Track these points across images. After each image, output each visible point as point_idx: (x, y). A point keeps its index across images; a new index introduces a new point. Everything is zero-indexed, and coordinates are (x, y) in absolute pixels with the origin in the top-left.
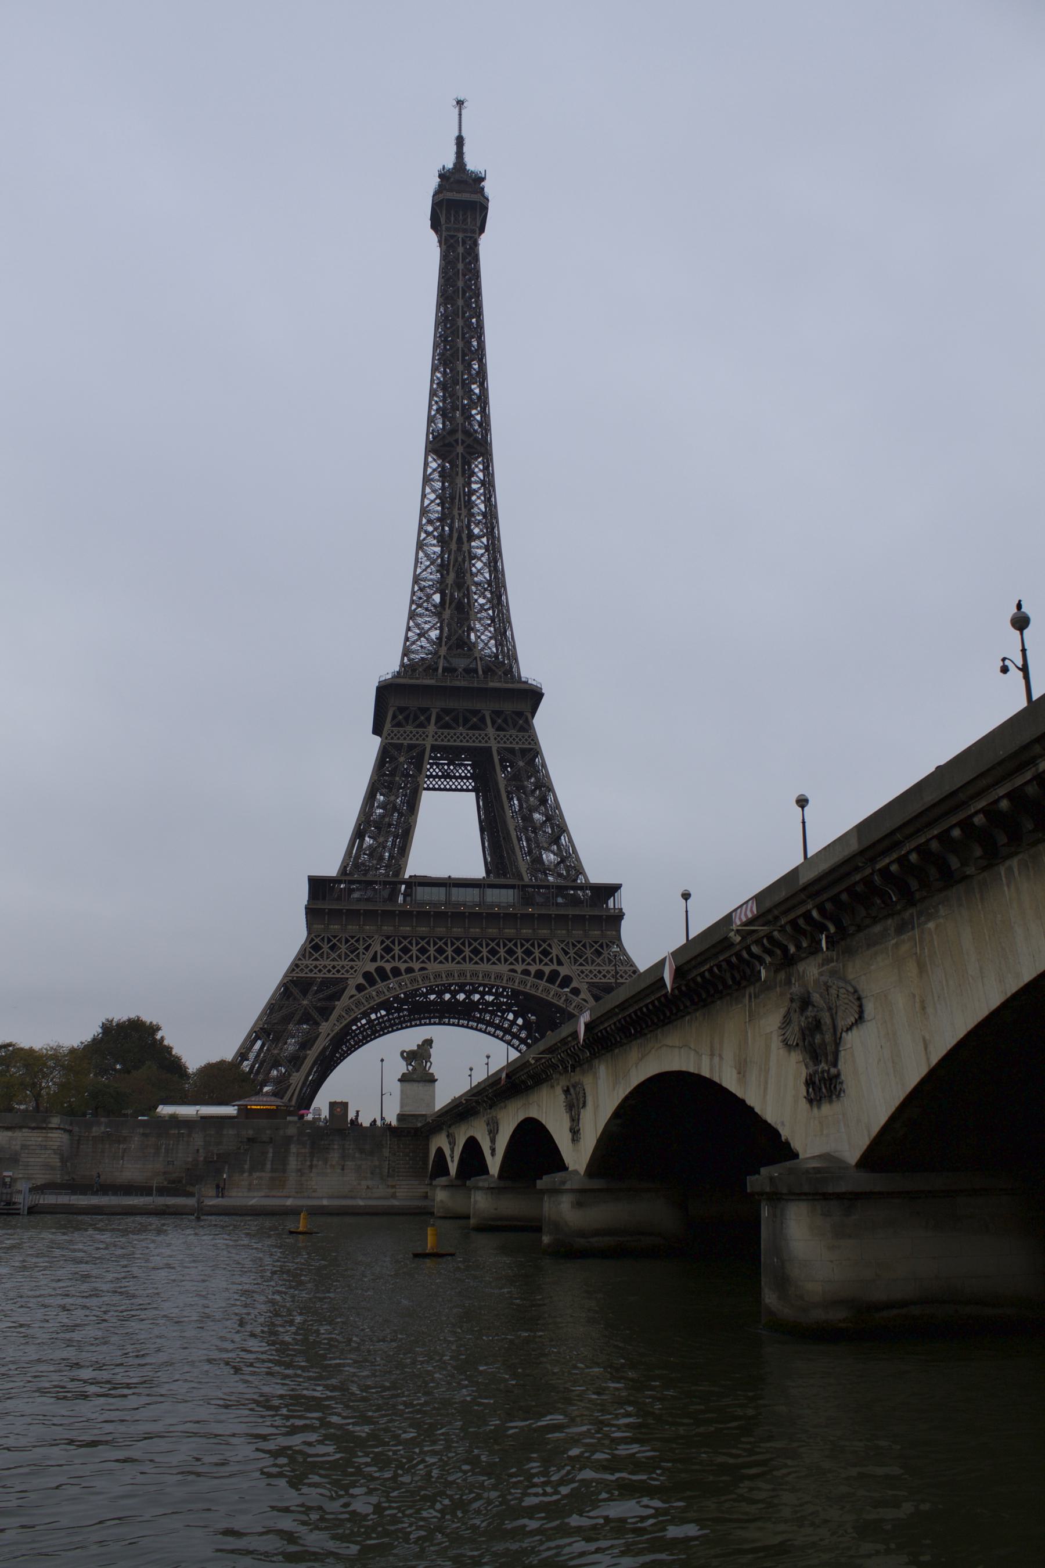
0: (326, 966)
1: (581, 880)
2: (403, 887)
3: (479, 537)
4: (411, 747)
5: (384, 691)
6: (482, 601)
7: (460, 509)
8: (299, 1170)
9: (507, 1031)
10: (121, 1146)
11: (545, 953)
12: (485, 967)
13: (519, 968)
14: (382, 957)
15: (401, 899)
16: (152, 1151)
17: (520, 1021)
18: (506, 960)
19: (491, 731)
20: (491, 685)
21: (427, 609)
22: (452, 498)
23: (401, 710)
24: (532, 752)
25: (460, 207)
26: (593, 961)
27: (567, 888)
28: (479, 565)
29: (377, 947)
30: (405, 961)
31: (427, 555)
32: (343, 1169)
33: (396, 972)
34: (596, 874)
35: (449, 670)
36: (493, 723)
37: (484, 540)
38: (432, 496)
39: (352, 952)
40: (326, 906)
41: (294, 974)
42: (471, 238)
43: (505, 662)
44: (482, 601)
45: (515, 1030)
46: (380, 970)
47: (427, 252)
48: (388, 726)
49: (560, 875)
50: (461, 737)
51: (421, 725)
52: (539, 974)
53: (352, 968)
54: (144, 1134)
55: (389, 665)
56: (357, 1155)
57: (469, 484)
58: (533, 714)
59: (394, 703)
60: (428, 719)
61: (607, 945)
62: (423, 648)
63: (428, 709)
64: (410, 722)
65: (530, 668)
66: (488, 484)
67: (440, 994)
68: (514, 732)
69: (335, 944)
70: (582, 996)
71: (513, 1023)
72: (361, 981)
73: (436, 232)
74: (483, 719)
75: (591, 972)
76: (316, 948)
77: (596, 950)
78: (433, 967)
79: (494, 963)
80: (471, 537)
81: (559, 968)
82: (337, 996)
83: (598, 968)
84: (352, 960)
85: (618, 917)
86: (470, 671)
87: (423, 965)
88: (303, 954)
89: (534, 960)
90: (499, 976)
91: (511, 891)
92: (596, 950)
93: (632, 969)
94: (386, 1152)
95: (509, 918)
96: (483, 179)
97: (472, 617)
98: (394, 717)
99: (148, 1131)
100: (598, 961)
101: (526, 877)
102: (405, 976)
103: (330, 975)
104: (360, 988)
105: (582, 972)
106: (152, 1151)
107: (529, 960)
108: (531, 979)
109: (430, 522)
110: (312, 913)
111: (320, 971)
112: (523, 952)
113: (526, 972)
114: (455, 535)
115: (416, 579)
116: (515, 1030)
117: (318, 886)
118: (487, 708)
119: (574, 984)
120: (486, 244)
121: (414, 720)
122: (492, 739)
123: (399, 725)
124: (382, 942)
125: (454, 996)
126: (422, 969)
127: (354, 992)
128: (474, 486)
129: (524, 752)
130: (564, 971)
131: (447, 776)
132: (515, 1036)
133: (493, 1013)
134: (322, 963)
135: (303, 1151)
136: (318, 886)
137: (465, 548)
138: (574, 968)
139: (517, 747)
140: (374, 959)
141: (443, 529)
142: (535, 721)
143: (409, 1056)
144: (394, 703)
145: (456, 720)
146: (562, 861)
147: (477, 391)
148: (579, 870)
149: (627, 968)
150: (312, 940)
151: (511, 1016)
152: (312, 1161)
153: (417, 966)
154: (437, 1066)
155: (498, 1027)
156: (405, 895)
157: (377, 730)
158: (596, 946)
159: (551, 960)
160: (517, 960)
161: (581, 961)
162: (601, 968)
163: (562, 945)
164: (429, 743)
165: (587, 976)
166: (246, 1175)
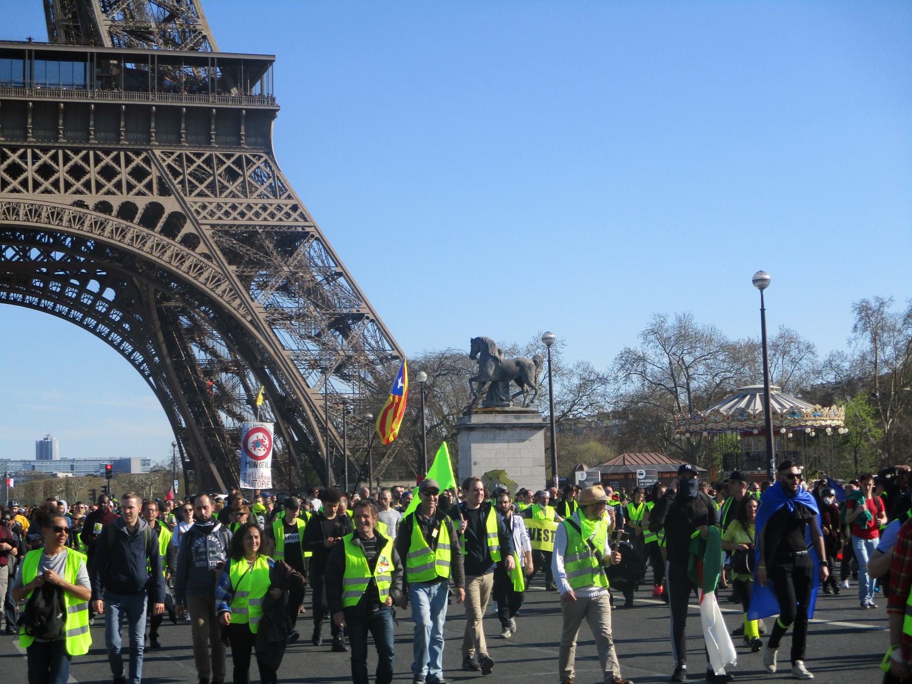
11: (140, 174)
12: (29, 197)
13: (91, 199)
18: (68, 186)
26: (223, 188)
27: (176, 61)
52: (127, 211)
61: (249, 161)
70: (202, 248)
75: (219, 206)
77: (229, 170)
79: (46, 191)
81: (162, 200)
83: (231, 201)
89: (118, 186)
90: (56, 214)
91: (79, 66)
92: (229, 170)
93: (291, 202)
100: (233, 187)
101: (107, 42)
107: (109, 186)
108: (113, 221)
112: (100, 173)
113: (104, 207)
130: (170, 205)
133: (46, 278)
149: (282, 201)
158: (229, 163)
159: (149, 186)
160: (87, 185)
161: (202, 187)
162: (235, 201)
163: (169, 161)
165: (212, 214)
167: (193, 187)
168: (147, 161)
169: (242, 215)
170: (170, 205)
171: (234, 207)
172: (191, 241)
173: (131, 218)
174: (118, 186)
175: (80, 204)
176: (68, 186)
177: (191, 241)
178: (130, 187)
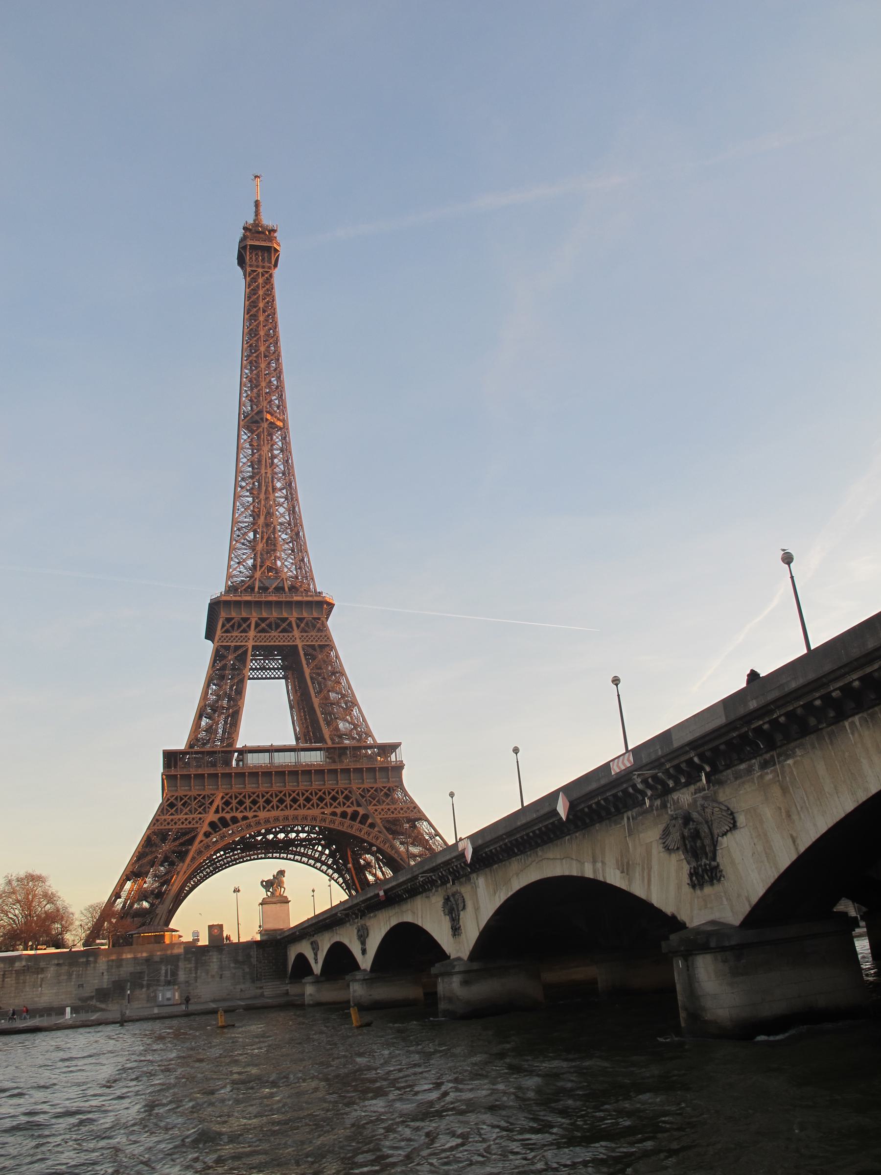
0: (181, 819)
1: (370, 741)
2: (236, 754)
3: (281, 490)
4: (237, 648)
5: (215, 607)
6: (284, 536)
7: (266, 468)
8: (187, 982)
9: (317, 860)
10: (40, 976)
11: (347, 798)
14: (223, 809)
15: (234, 763)
16: (66, 977)
17: (327, 852)
19: (296, 633)
20: (296, 598)
21: (243, 544)
22: (260, 461)
23: (228, 620)
24: (327, 646)
25: (257, 251)
26: (384, 802)
27: (360, 748)
28: (282, 510)
29: (218, 802)
30: (241, 812)
31: (242, 505)
32: (221, 978)
33: (235, 820)
34: (381, 737)
35: (264, 589)
36: (298, 626)
37: (284, 491)
38: (245, 460)
39: (200, 807)
40: (179, 772)
41: (156, 827)
42: (267, 272)
43: (302, 581)
44: (284, 536)
45: (323, 859)
46: (222, 820)
47: (236, 282)
48: (219, 632)
49: (354, 738)
50: (275, 638)
51: (244, 631)
53: (200, 819)
54: (58, 965)
55: (218, 589)
56: (232, 965)
57: (271, 450)
58: (327, 618)
59: (223, 615)
60: (249, 626)
62: (242, 573)
63: (248, 619)
64: (236, 628)
65: (324, 584)
66: (286, 450)
67: (264, 835)
68: (314, 633)
69: (186, 802)
70: (376, 829)
71: (322, 853)
72: (210, 830)
73: (242, 267)
74: (290, 625)
76: (172, 805)
78: (262, 815)
79: (309, 808)
80: (274, 489)
81: (358, 809)
82: (191, 841)
84: (200, 813)
85: (399, 767)
86: (279, 589)
87: (255, 814)
88: (162, 810)
94: (254, 961)
95: (320, 772)
96: (275, 231)
97: (279, 548)
98: (223, 625)
99: (61, 962)
102: (242, 823)
103: (184, 826)
104: (207, 835)
105: (376, 810)
106: (66, 977)
108: (338, 819)
109: (243, 479)
110: (169, 778)
111: (175, 823)
113: (334, 814)
114: (264, 489)
115: (234, 522)
116: (323, 859)
117: (171, 758)
118: (293, 616)
119: (370, 821)
120: (278, 275)
121: (238, 628)
122: (298, 639)
123: (227, 631)
124: (223, 798)
125: (275, 836)
126: (255, 816)
127: (204, 838)
128: (276, 452)
129: (322, 647)
130: (362, 811)
131: (263, 668)
132: (323, 863)
134: (176, 817)
135: (189, 966)
136: (171, 758)
137: (272, 497)
138: (370, 808)
139: (317, 644)
140: (217, 811)
141: (254, 483)
142: (329, 623)
143: (267, 885)
144: (221, 616)
145: (270, 625)
146: (355, 728)
147: (275, 383)
148: (369, 734)
150: (168, 799)
151: (320, 848)
152: (196, 973)
153: (250, 814)
154: (290, 888)
155: (310, 857)
156: (238, 761)
157: (210, 635)
159: (352, 803)
161: (374, 802)
164: (250, 644)
166: (144, 990)
167: (371, 802)
168: (350, 792)
169: (393, 812)
170: (362, 811)
171: (389, 809)
172: (372, 826)
173: (346, 818)
174: (339, 804)
175: (323, 813)
176: (318, 805)
177: (372, 826)
178: (344, 804)
